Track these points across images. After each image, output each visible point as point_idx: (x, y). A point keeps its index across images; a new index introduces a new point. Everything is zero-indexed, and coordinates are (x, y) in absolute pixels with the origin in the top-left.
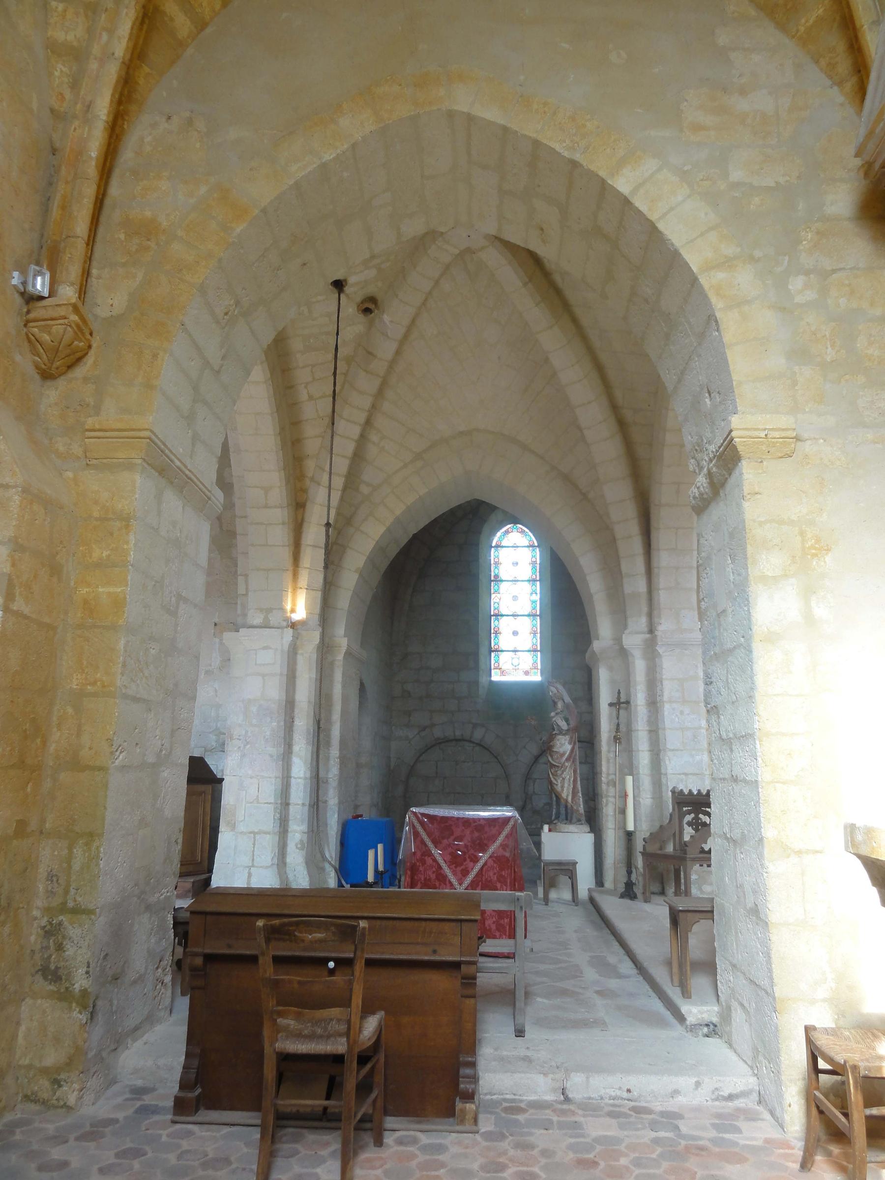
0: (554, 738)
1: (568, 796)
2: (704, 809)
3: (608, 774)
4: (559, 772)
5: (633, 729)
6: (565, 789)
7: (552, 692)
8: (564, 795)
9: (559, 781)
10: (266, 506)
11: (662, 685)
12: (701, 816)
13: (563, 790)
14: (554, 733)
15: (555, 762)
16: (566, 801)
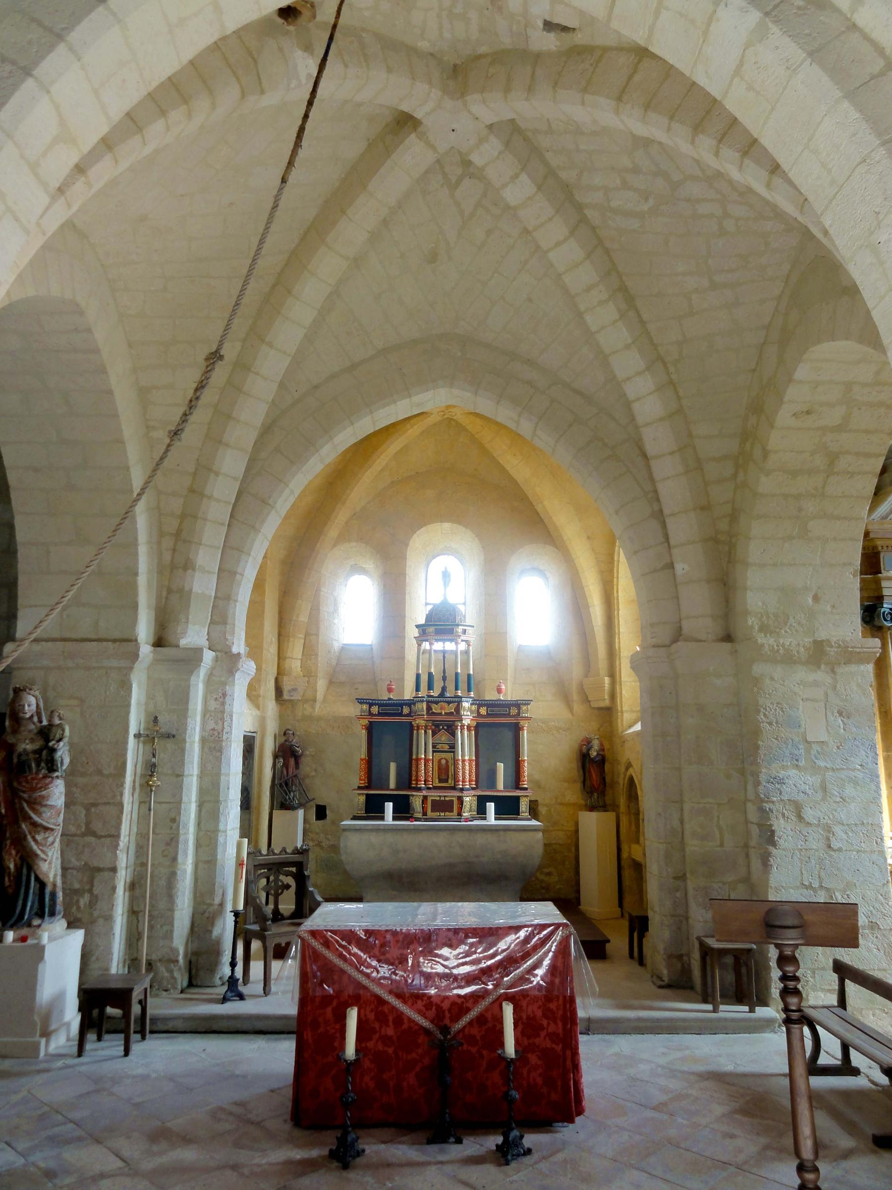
0: (47, 785)
1: (55, 876)
2: (287, 869)
3: (125, 837)
4: (51, 839)
5: (186, 773)
6: (53, 866)
7: (29, 706)
8: (51, 876)
9: (50, 854)
10: (34, 167)
11: (232, 720)
12: (282, 877)
13: (50, 868)
14: (56, 774)
15: (48, 823)
16: (55, 885)
